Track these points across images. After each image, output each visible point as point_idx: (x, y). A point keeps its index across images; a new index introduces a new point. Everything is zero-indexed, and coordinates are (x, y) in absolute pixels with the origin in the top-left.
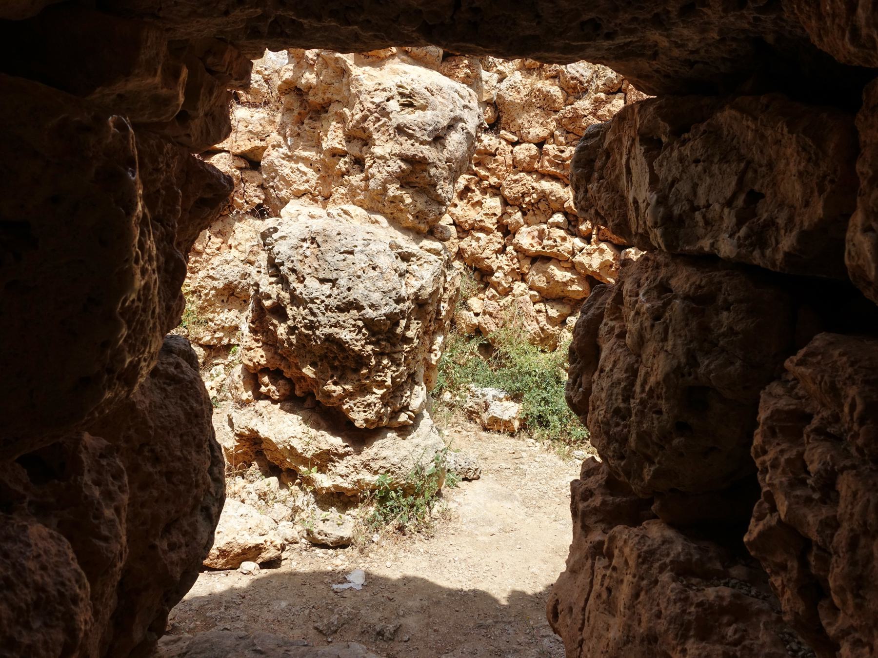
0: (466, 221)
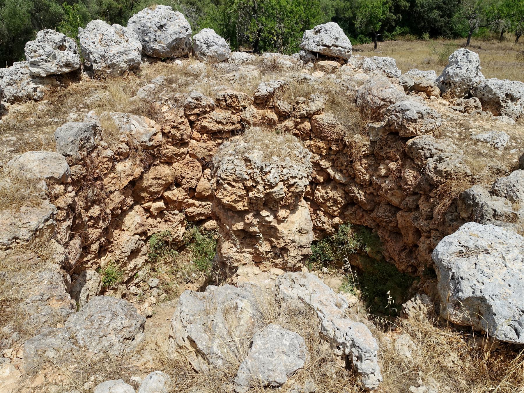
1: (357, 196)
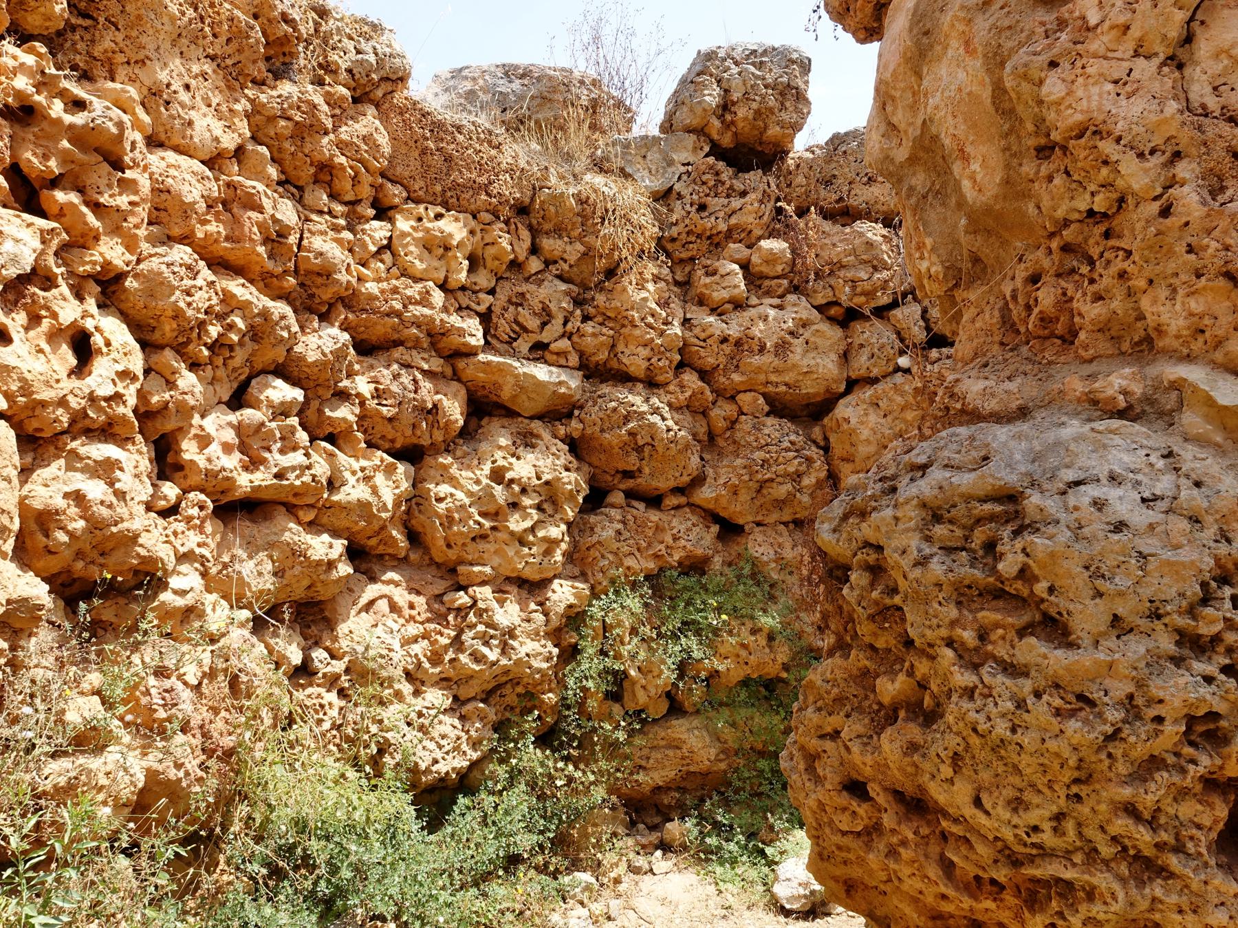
0: (62, 402)
1: (652, 426)
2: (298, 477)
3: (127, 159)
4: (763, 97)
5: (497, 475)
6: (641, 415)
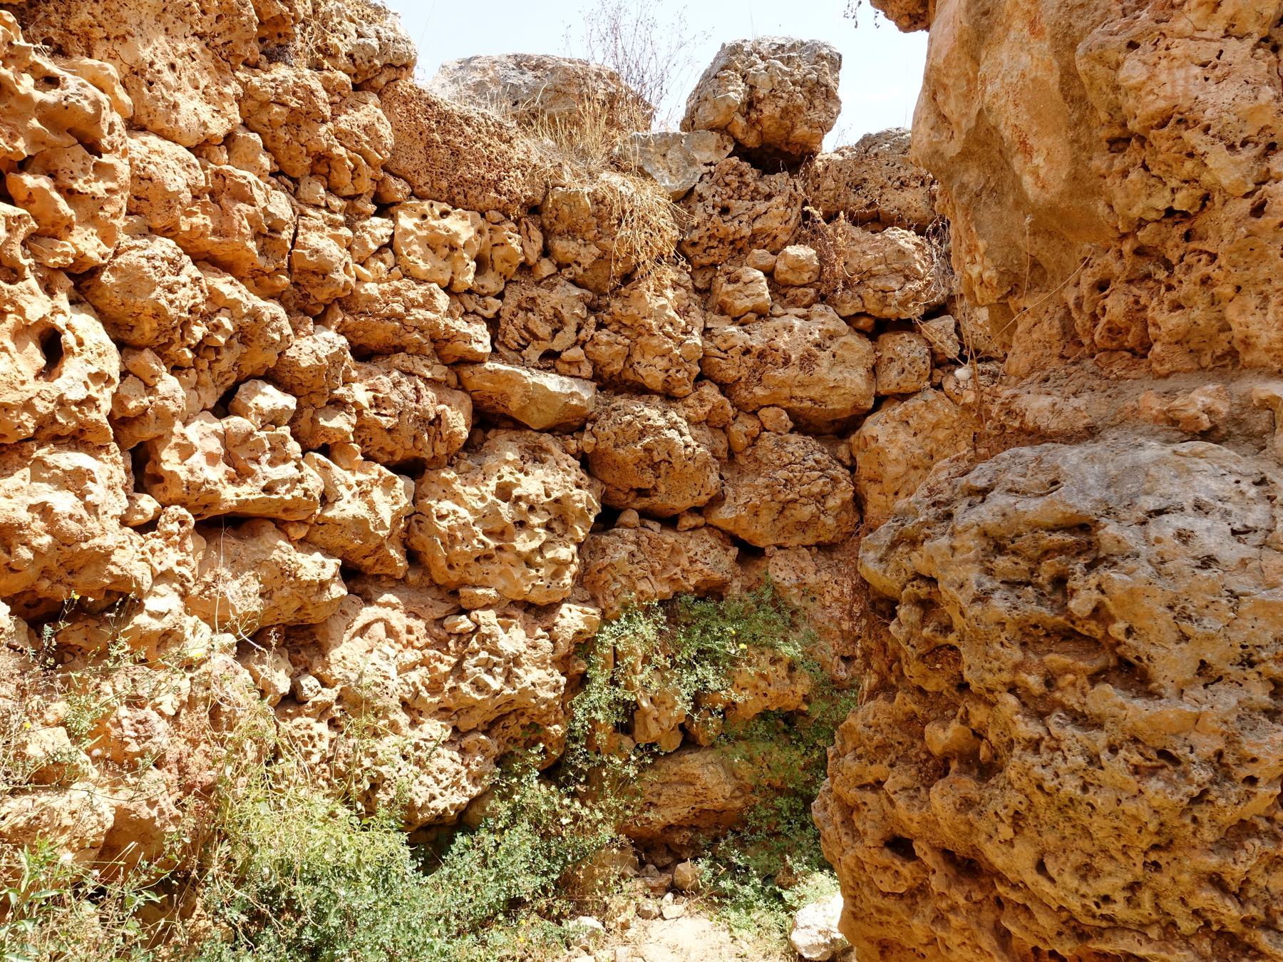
0: (28, 406)
1: (669, 441)
2: (288, 491)
3: (104, 142)
4: (791, 94)
5: (504, 492)
6: (658, 430)
